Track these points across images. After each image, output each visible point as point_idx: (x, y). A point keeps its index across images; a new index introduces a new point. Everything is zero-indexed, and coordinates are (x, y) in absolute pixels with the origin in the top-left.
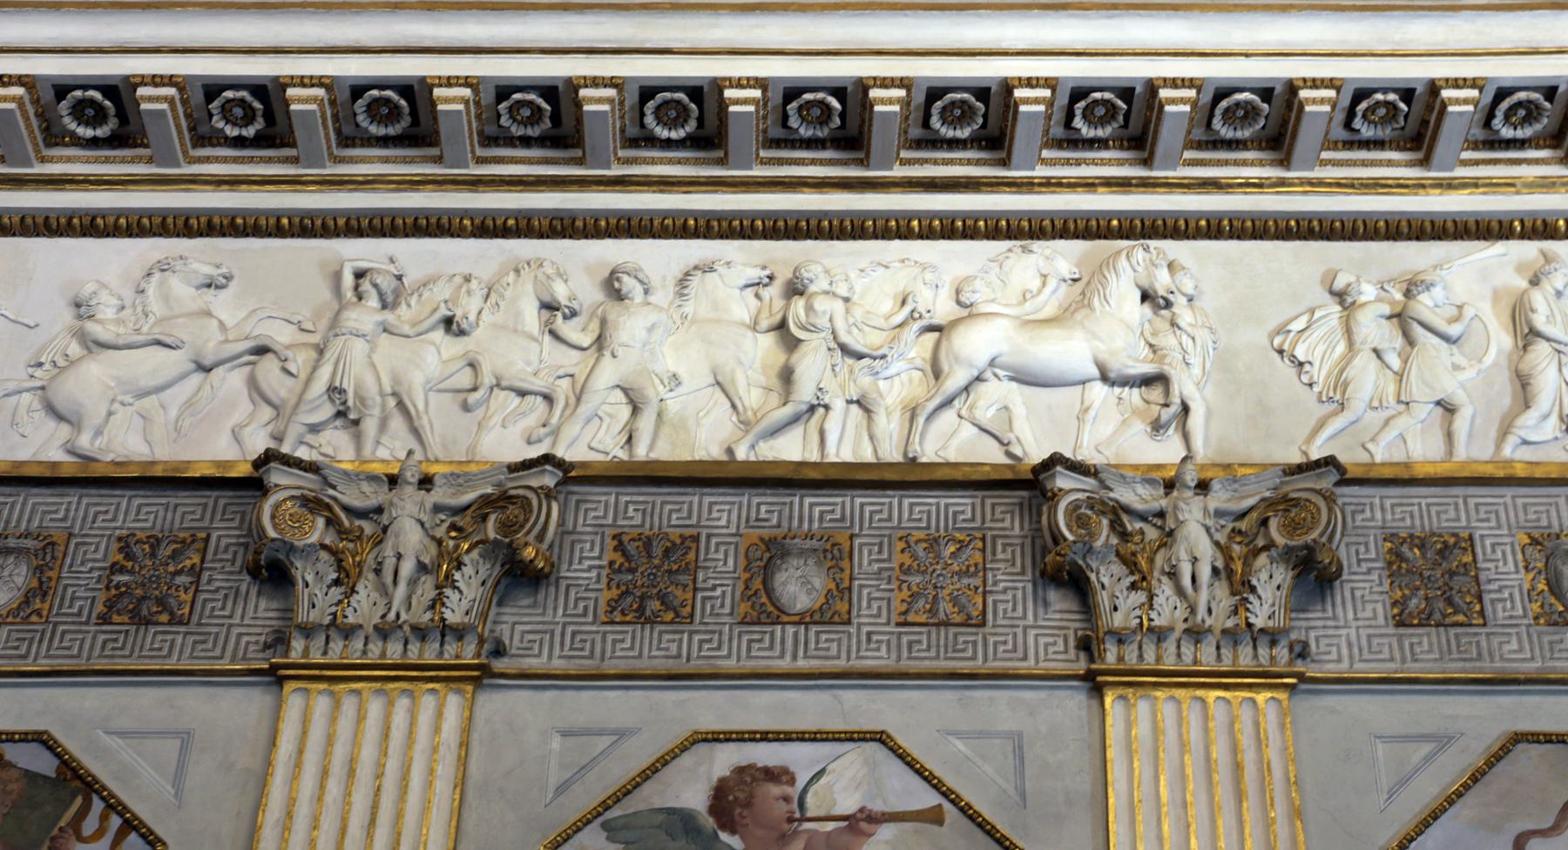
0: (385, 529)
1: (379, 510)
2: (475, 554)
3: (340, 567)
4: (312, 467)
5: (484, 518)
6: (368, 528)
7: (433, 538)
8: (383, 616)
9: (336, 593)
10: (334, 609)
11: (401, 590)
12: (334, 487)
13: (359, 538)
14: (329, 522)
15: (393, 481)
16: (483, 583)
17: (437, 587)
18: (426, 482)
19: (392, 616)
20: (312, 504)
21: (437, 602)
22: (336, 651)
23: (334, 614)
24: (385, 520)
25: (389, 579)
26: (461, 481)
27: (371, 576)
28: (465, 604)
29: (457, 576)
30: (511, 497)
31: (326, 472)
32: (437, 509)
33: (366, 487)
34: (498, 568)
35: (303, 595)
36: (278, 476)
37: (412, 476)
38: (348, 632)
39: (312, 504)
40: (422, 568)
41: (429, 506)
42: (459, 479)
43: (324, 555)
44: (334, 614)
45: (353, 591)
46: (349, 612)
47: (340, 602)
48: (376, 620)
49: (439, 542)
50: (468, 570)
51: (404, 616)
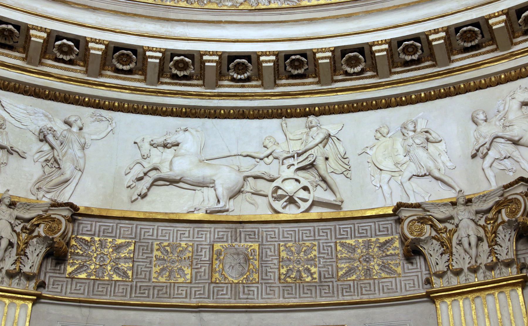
0: (457, 226)
1: (452, 218)
2: (501, 228)
3: (442, 244)
4: (418, 206)
5: (499, 212)
6: (450, 227)
7: (480, 225)
8: (470, 263)
9: (446, 257)
10: (447, 264)
11: (474, 249)
12: (429, 211)
13: (446, 231)
14: (431, 226)
15: (454, 204)
16: (509, 240)
17: (489, 247)
18: (469, 202)
19: (473, 262)
20: (422, 220)
21: (492, 252)
22: (455, 282)
23: (448, 266)
24: (456, 221)
25: (466, 246)
26: (484, 198)
27: (458, 247)
28: (506, 251)
30: (510, 200)
31: (424, 206)
32: (477, 212)
33: (442, 209)
34: (513, 233)
35: (432, 260)
36: (404, 213)
37: (461, 201)
38: (458, 273)
39: (422, 220)
40: (480, 239)
41: (474, 212)
42: (484, 197)
43: (434, 241)
44: (448, 266)
45: (451, 254)
46: (454, 263)
47: (449, 260)
48: (467, 266)
49: (484, 227)
50: (501, 235)
51: (479, 262)
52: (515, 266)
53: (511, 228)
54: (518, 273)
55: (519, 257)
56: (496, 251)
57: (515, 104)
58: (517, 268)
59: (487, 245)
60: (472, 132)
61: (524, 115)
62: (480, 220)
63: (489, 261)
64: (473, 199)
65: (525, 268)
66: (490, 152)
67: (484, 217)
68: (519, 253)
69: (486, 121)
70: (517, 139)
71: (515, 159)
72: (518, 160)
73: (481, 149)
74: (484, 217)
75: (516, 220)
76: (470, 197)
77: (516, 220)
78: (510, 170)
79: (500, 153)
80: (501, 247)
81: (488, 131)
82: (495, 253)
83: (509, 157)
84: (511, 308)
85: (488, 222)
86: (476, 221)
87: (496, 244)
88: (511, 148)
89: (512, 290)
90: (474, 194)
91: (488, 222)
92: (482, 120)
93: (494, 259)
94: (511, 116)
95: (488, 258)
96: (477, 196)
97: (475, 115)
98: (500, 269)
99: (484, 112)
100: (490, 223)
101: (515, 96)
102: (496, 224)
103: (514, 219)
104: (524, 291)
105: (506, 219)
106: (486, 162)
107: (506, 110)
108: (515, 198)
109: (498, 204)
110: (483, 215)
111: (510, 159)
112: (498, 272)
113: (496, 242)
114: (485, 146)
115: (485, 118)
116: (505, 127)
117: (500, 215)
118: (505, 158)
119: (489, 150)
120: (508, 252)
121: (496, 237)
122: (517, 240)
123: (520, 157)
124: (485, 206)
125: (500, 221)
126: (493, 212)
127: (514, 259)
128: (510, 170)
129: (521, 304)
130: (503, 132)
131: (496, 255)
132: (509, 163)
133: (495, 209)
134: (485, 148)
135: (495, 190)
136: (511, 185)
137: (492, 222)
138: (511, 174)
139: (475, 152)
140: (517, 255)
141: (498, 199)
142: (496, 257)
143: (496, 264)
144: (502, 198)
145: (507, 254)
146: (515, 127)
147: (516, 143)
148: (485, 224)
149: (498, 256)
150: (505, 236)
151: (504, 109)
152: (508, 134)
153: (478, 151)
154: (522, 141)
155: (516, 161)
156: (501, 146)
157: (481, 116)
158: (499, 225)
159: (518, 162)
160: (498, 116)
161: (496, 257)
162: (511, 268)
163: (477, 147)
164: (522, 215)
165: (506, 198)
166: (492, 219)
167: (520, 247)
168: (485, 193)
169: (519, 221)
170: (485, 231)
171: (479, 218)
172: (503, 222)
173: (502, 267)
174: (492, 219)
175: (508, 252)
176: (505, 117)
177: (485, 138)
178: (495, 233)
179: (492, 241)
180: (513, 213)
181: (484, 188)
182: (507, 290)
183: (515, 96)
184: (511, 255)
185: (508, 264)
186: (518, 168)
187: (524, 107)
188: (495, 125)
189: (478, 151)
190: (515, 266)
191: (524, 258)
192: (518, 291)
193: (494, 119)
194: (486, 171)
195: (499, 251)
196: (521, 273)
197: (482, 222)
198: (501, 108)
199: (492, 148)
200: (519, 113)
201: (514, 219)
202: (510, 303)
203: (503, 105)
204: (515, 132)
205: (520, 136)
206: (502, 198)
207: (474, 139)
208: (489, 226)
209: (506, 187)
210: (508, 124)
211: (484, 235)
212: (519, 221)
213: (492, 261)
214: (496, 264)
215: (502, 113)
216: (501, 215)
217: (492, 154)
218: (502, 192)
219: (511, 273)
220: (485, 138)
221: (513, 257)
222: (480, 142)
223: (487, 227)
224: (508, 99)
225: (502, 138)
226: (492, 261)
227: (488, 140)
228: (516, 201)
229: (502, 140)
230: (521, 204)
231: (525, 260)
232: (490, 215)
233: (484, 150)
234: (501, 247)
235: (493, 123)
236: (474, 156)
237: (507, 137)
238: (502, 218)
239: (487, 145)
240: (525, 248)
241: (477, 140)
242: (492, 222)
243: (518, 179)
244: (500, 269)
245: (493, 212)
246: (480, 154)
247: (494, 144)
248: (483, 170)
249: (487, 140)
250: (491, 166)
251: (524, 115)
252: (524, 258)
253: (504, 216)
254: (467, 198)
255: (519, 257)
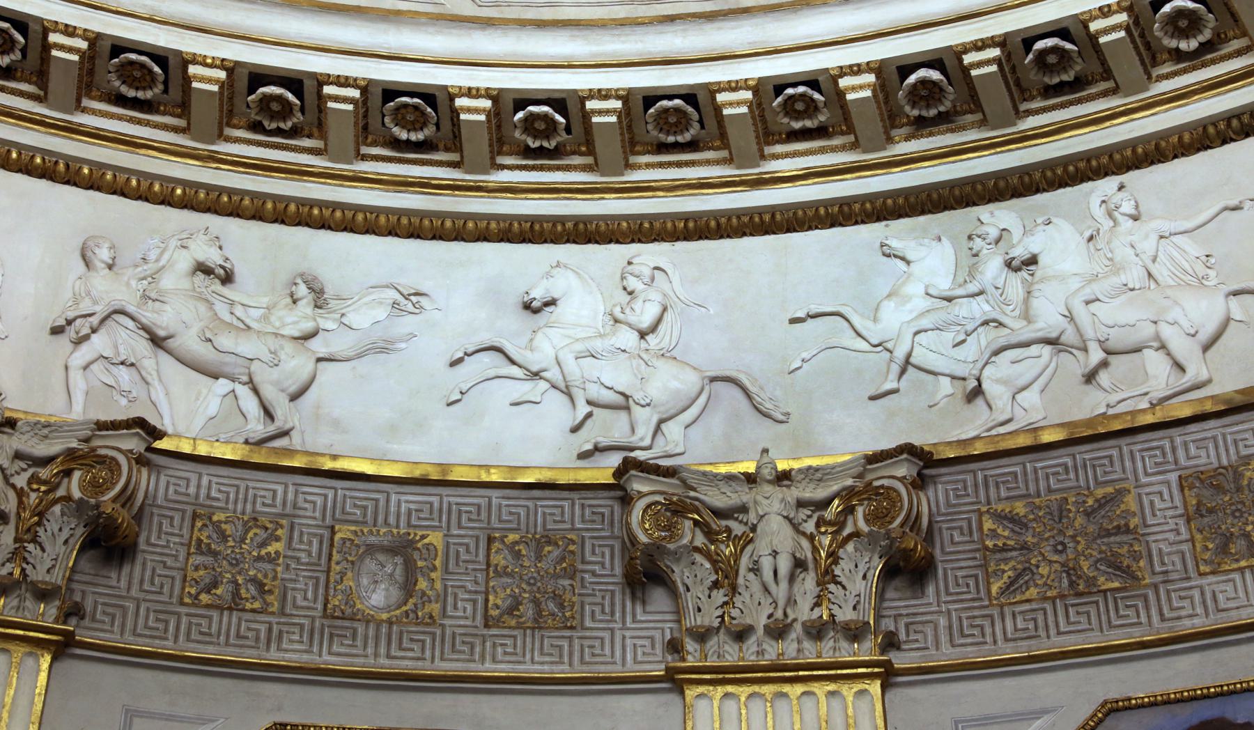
2: (57, 509)
5: (68, 473)
7: (13, 486)
16: (66, 542)
17: (16, 540)
26: (46, 431)
28: (48, 564)
29: (41, 531)
34: (80, 531)
41: (11, 453)
42: (47, 428)
49: (20, 493)
50: (52, 525)
52: (57, 603)
53: (79, 518)
54: (56, 621)
55: (75, 586)
56: (27, 555)
57: (184, 262)
58: (60, 608)
59: (13, 535)
60: (72, 277)
61: (194, 290)
62: (18, 473)
63: (4, 572)
64: (19, 424)
65: (76, 615)
66: (94, 336)
67: (31, 471)
68: (77, 577)
69: (110, 267)
70: (162, 333)
71: (144, 373)
72: (149, 379)
73: (78, 321)
74: (31, 471)
75: (97, 506)
76: (15, 415)
77: (97, 506)
78: (123, 393)
79: (116, 347)
80: (43, 550)
81: (108, 290)
82: (25, 559)
83: (132, 365)
84: (12, 692)
85: (35, 486)
86: (8, 472)
87: (34, 540)
88: (142, 346)
89: (30, 654)
90: (26, 412)
91: (35, 486)
92: (103, 262)
93: (17, 572)
94: (168, 282)
95: (3, 565)
96: (32, 419)
97: (90, 243)
98: (22, 599)
99: (112, 247)
100: (38, 490)
101: (190, 243)
102: (51, 496)
103: (93, 501)
104: (56, 665)
105: (77, 494)
106: (77, 354)
107: (161, 264)
108: (113, 459)
109: (71, 454)
110: (30, 466)
111: (133, 369)
112: (15, 603)
113: (36, 535)
114: (91, 319)
115: (110, 262)
116: (145, 297)
117: (66, 480)
118: (122, 363)
119: (94, 331)
120: (54, 566)
121: (39, 524)
122: (82, 550)
123: (154, 373)
124: (43, 449)
125: (61, 492)
126: (54, 469)
127: (60, 588)
128: (123, 393)
129: (37, 691)
130: (138, 307)
131: (24, 565)
132: (127, 377)
133: (62, 463)
134: (87, 325)
135: (75, 423)
136: (114, 425)
137: (43, 488)
138: (124, 402)
139: (62, 322)
140: (70, 580)
141: (74, 445)
142: (23, 570)
143: (17, 584)
144: (83, 446)
145: (48, 571)
146: (167, 307)
147: (157, 341)
148: (26, 488)
149: (29, 568)
150: (60, 530)
151: (157, 260)
152: (148, 315)
153: (69, 322)
154: (170, 343)
155: (143, 378)
156: (123, 333)
157: (104, 254)
158: (56, 501)
159: (147, 383)
160: (140, 269)
161: (23, 570)
162: (46, 604)
163: (71, 315)
164: (114, 500)
165: (93, 450)
166: (45, 483)
167: (85, 565)
168: (53, 420)
169: (102, 509)
170: (20, 503)
171: (17, 468)
172: (68, 498)
173: (28, 595)
174: (45, 483)
175: (54, 566)
176: (153, 277)
177: (95, 302)
178: (41, 515)
179: (29, 530)
180: (96, 487)
181: (52, 406)
182: (19, 650)
183: (190, 243)
184: (58, 578)
185: (43, 594)
186: (143, 395)
187: (201, 276)
188: (128, 284)
189: (69, 322)
190: (57, 603)
191: (83, 592)
192: (42, 660)
193: (130, 271)
194: (72, 373)
195: (35, 558)
196: (65, 623)
197: (21, 481)
198: (152, 256)
199: (102, 331)
200: (185, 284)
201: (93, 501)
202: (14, 680)
203: (159, 251)
204: (163, 319)
205: (171, 331)
206: (83, 446)
207: (71, 295)
208: (33, 496)
209: (102, 426)
210: (153, 295)
211: (14, 510)
212: (102, 509)
213: (11, 574)
214: (17, 584)
215: (150, 267)
216: (69, 482)
217: (99, 343)
218: (90, 433)
219: (43, 615)
220: (95, 302)
221: (59, 582)
222: (81, 306)
223: (28, 496)
224: (174, 243)
225: (133, 318)
226: (11, 574)
227: (101, 309)
228: (112, 466)
229: (130, 324)
230: (120, 475)
231: (83, 598)
232: (44, 473)
233: (83, 327)
234: (43, 550)
235: (126, 278)
236: (56, 331)
237: (144, 320)
238: (68, 489)
239: (95, 320)
240: (92, 572)
241: (76, 300)
242: (43, 488)
243: (133, 419)
244: (22, 599)
245: (54, 469)
246: (71, 332)
247: (109, 322)
248: (67, 368)
249: (97, 308)
250: (85, 368)
251: (194, 290)
252: (83, 592)
253: (74, 487)
254: (8, 414)
255: (75, 586)
